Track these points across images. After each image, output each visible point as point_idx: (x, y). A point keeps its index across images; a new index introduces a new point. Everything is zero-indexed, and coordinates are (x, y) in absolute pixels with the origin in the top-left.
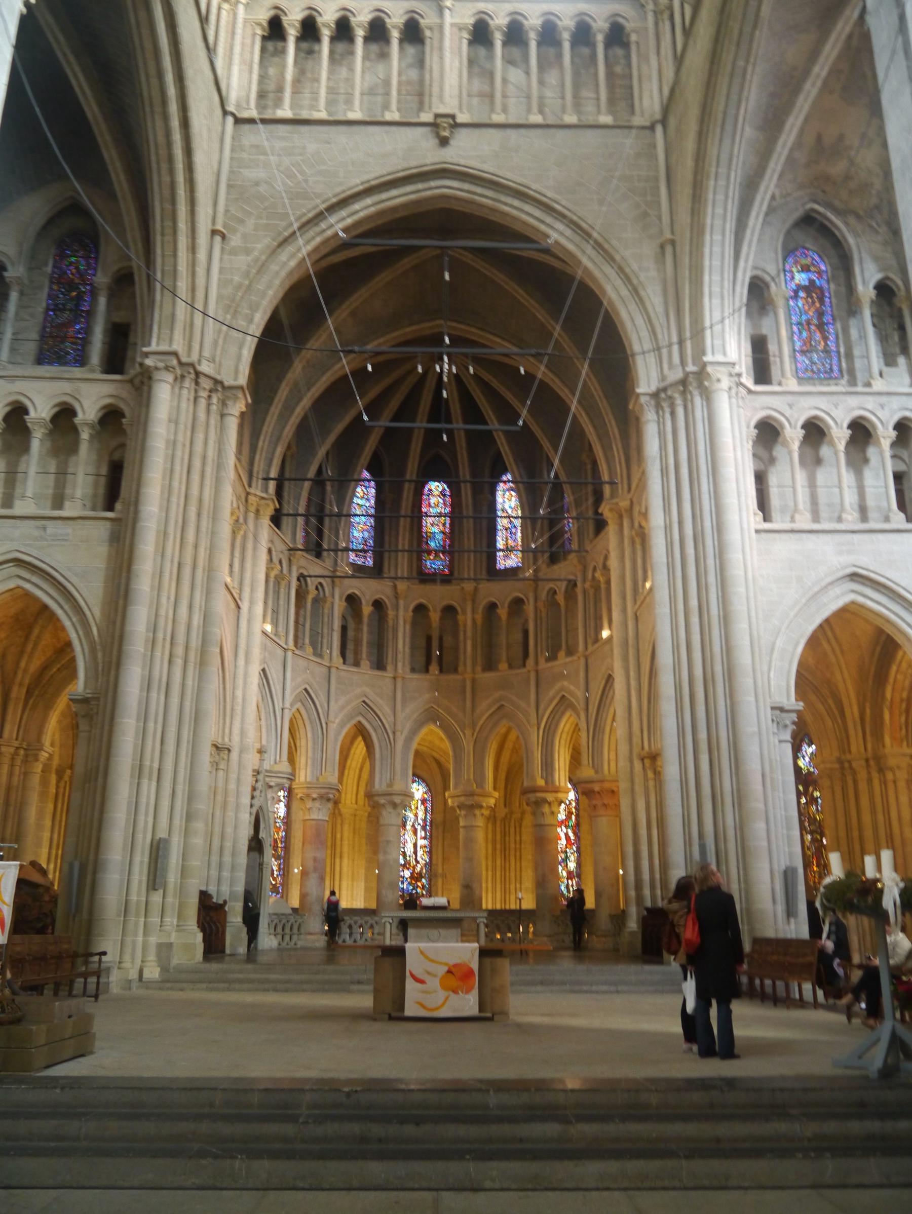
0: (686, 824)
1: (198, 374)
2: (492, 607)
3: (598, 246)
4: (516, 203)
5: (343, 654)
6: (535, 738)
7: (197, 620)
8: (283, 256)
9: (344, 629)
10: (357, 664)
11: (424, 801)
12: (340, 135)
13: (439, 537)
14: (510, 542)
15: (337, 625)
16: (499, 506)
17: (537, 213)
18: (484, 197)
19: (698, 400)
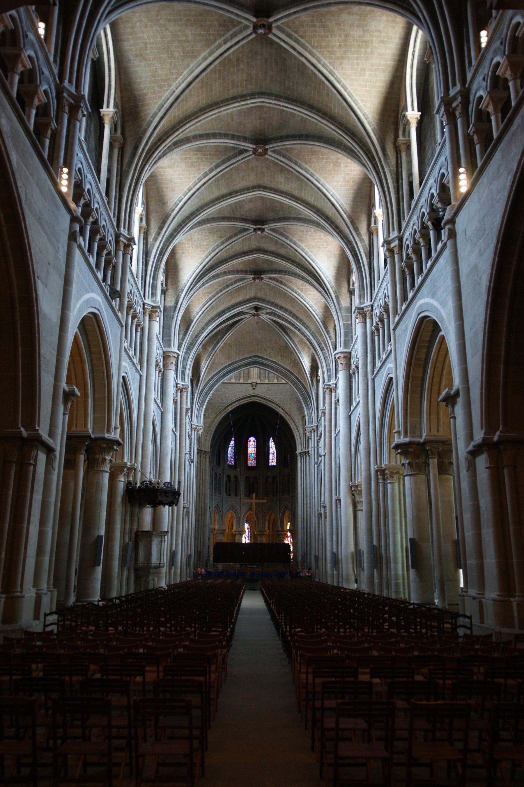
0: (302, 548)
1: (201, 451)
2: (267, 477)
3: (289, 415)
4: (271, 403)
5: (226, 492)
6: (279, 517)
7: (203, 505)
8: (217, 418)
9: (226, 484)
10: (229, 495)
11: (248, 529)
12: (230, 387)
13: (253, 455)
14: (273, 458)
15: (224, 484)
16: (270, 446)
17: (275, 406)
18: (263, 402)
19: (308, 457)
